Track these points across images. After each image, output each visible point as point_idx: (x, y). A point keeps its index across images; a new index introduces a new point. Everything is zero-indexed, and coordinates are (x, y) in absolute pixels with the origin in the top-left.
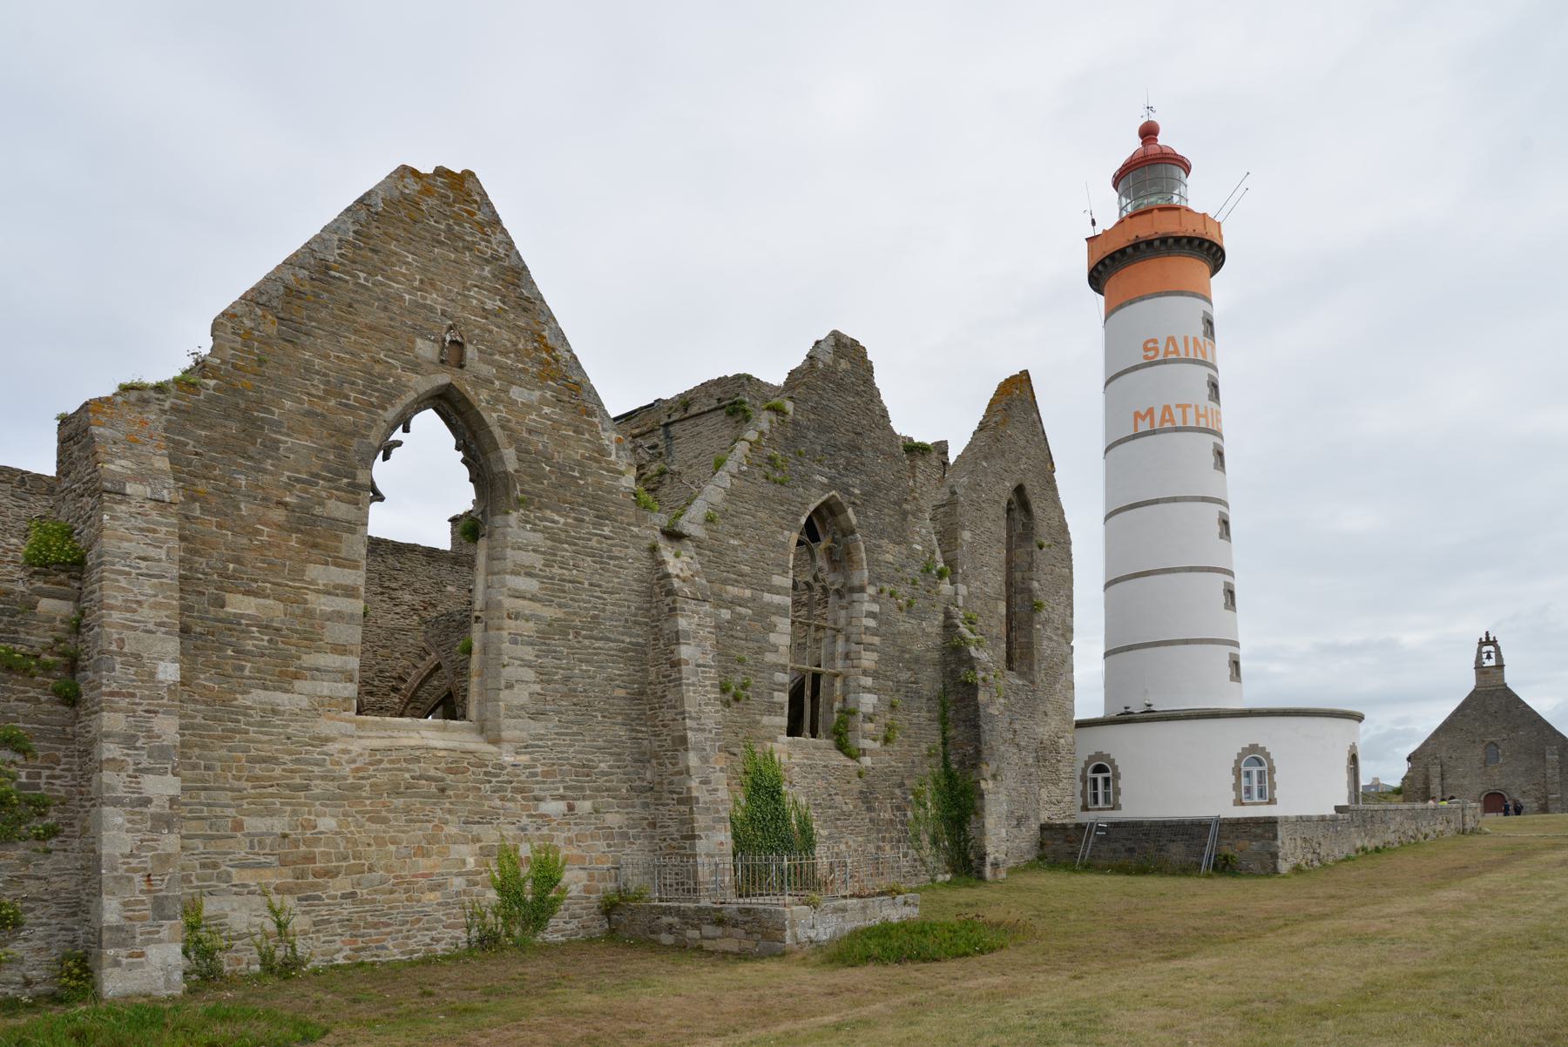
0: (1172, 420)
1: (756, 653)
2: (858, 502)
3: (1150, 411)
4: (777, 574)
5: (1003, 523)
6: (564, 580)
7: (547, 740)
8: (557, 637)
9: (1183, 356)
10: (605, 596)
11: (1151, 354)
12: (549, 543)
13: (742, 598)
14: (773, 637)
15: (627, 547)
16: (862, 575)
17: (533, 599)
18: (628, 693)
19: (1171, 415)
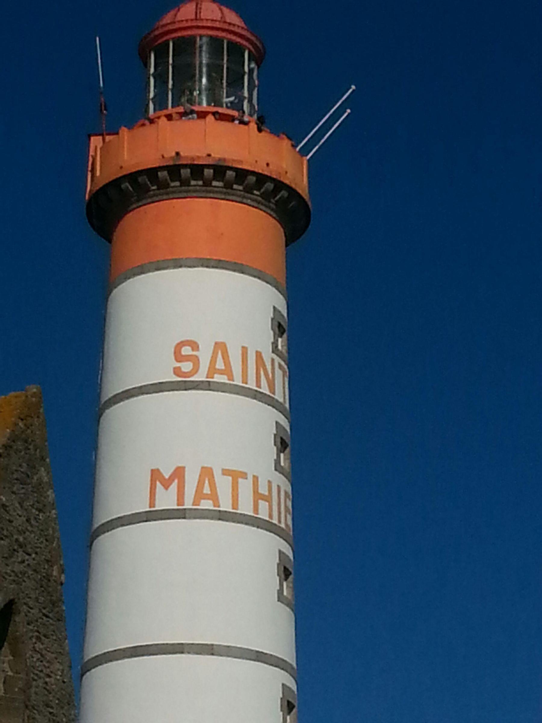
0: (214, 497)
9: (238, 381)
11: (186, 367)
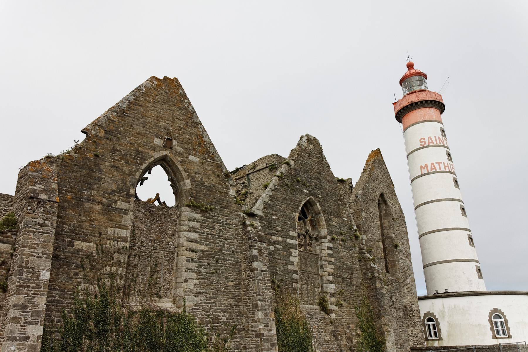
0: (435, 168)
1: (285, 265)
2: (321, 200)
3: (426, 165)
4: (292, 231)
5: (377, 209)
7: (201, 306)
8: (205, 259)
9: (435, 144)
10: (224, 240)
12: (202, 218)
13: (278, 241)
14: (291, 258)
15: (233, 220)
16: (324, 231)
17: (196, 242)
18: (234, 284)
19: (434, 166)
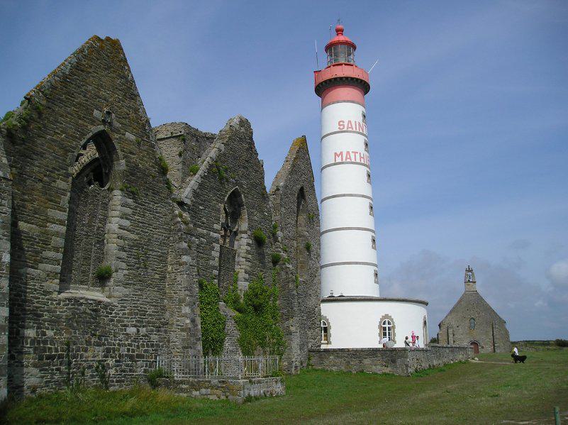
0: (350, 158)
3: (341, 153)
6: (139, 222)
11: (342, 127)
